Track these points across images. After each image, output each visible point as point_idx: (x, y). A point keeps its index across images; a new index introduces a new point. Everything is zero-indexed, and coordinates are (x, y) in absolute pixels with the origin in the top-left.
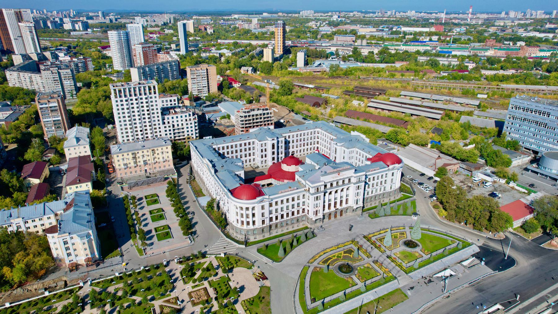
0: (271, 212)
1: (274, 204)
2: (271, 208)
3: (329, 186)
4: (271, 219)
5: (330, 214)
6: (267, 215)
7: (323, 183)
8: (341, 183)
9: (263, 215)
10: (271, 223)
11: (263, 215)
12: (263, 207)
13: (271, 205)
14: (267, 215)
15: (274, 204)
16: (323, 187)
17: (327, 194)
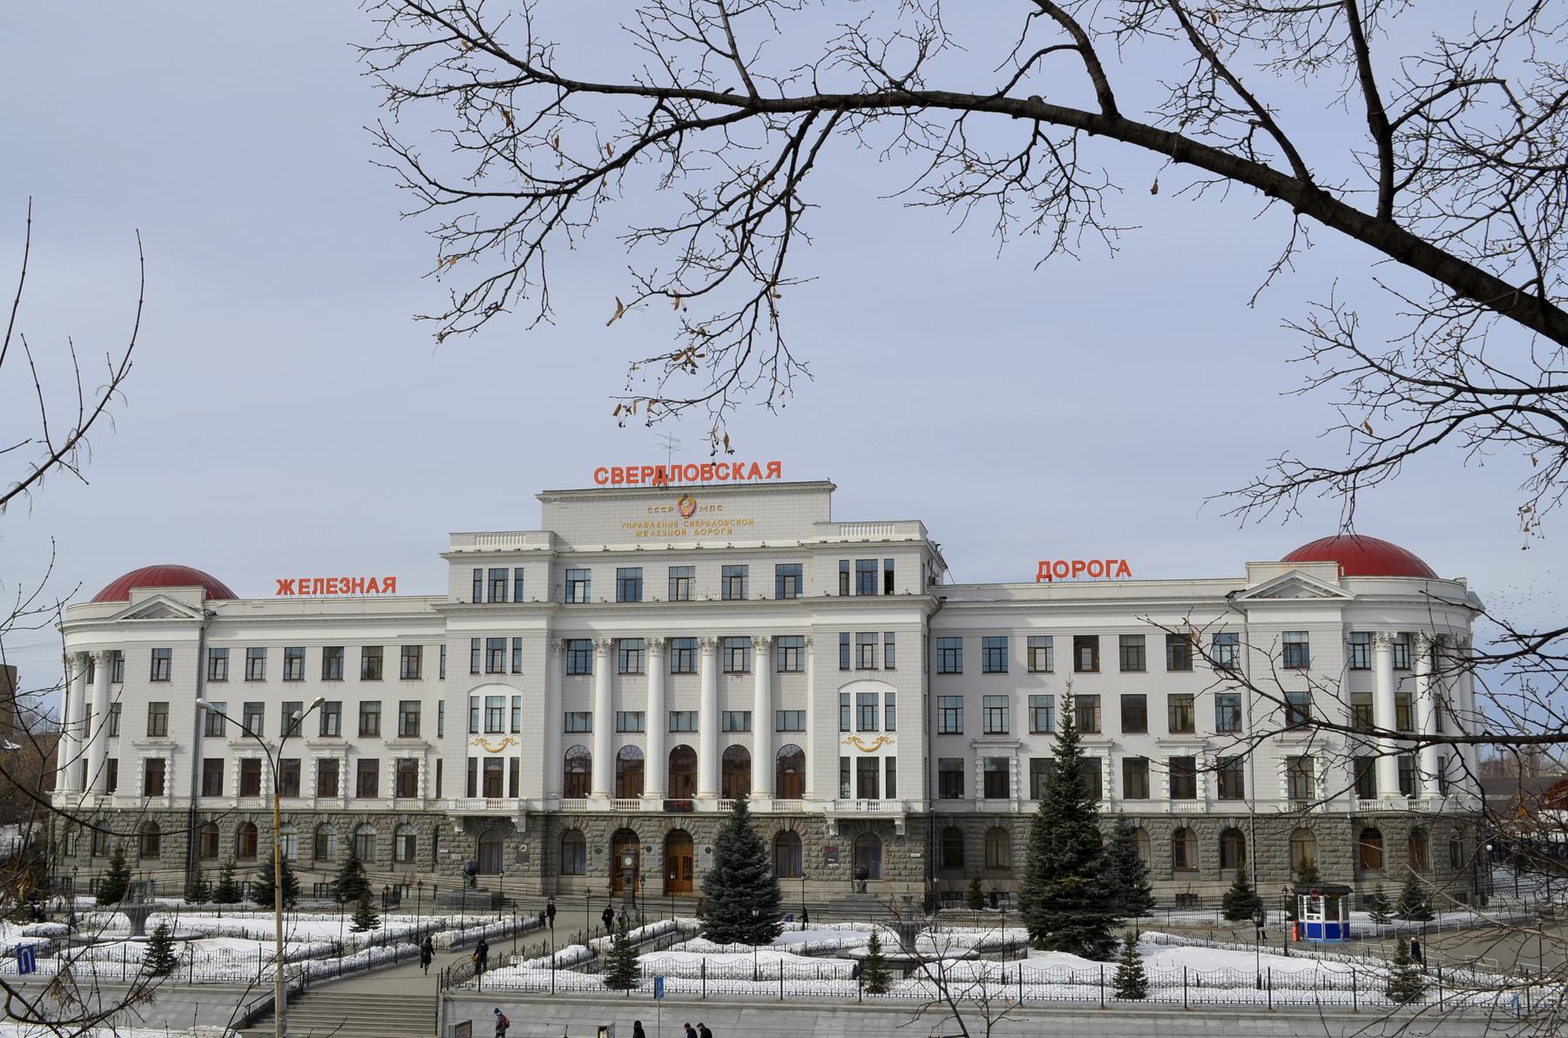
0: (211, 721)
1: (237, 664)
2: (214, 693)
3: (603, 584)
4: (211, 774)
5: (624, 837)
6: (181, 726)
7: (545, 546)
8: (708, 582)
9: (158, 716)
10: (207, 803)
11: (158, 716)
12: (161, 661)
13: (212, 665)
14: (181, 726)
15: (237, 664)
16: (537, 584)
17: (600, 664)
